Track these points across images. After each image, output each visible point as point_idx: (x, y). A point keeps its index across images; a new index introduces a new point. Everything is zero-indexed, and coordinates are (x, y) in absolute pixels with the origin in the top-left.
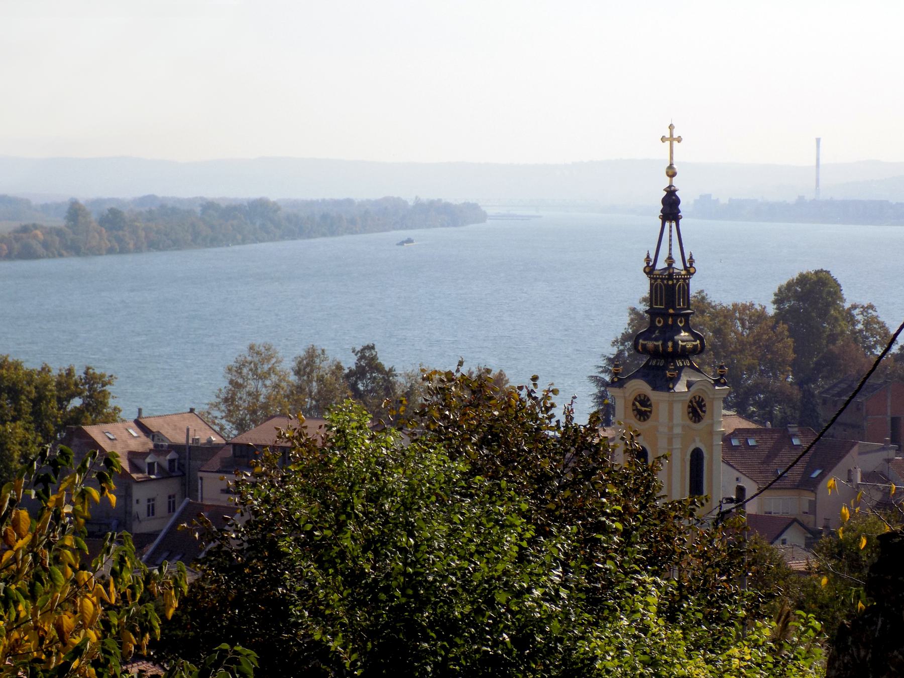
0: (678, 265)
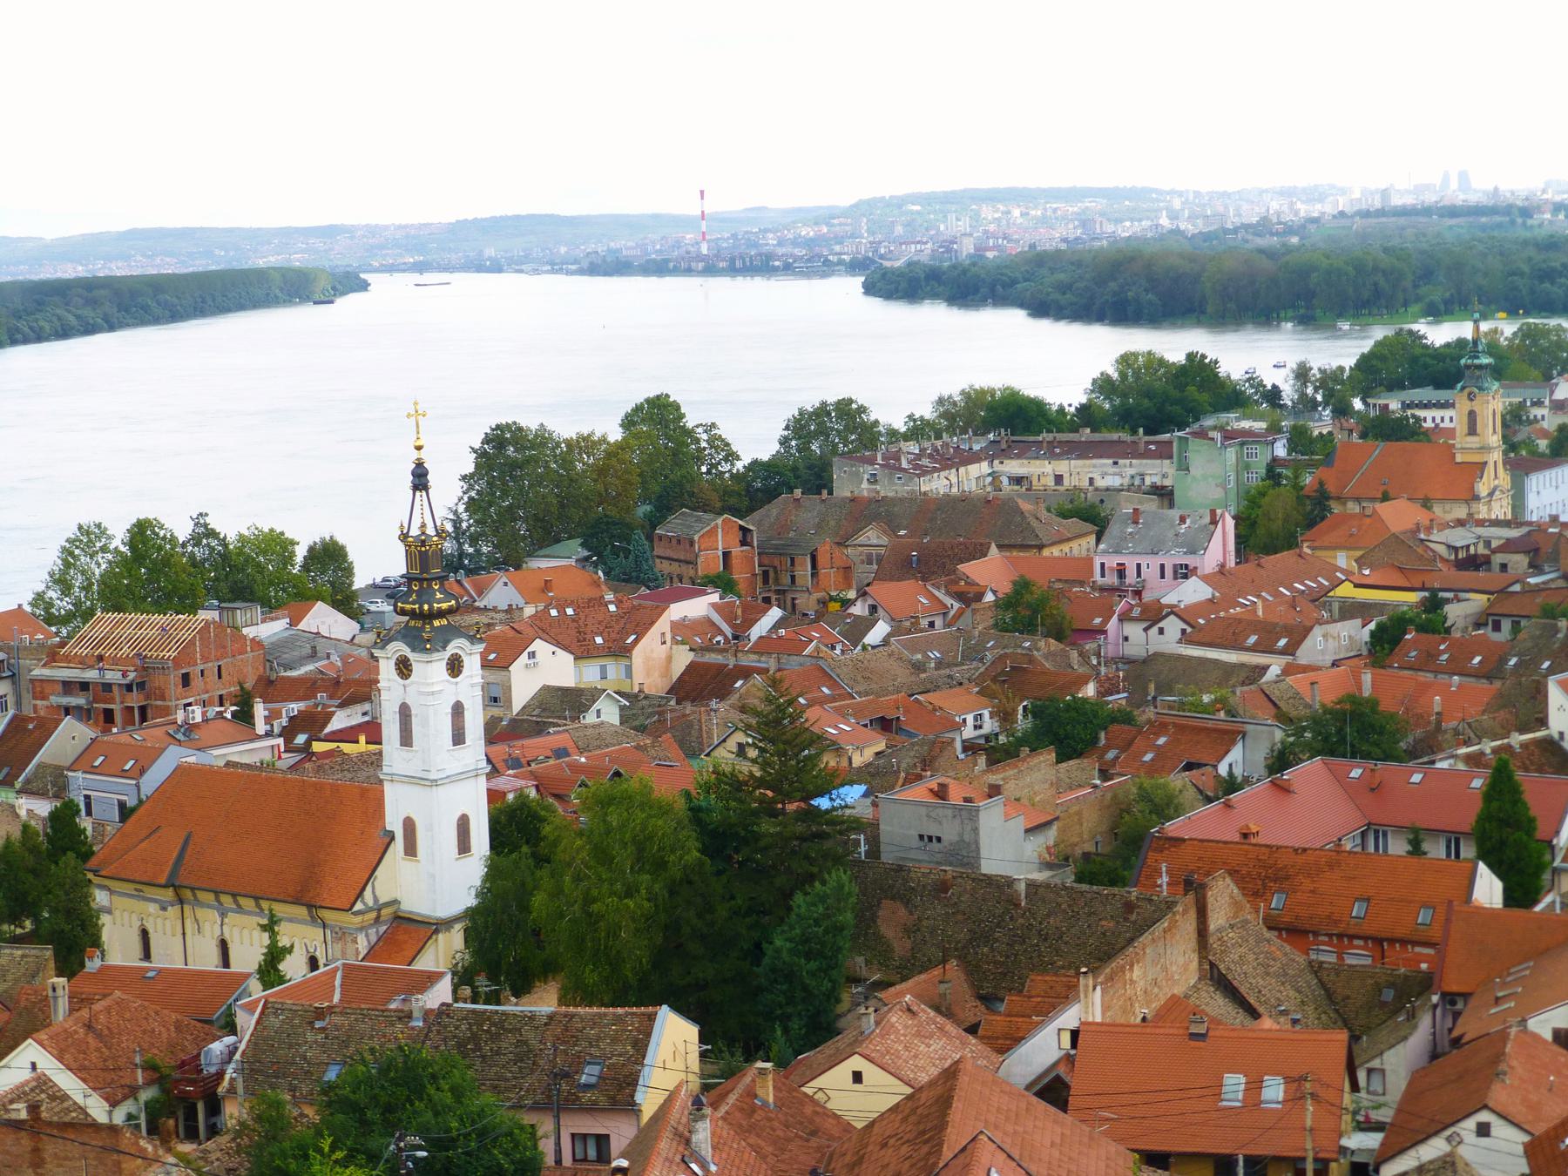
0: (430, 531)
